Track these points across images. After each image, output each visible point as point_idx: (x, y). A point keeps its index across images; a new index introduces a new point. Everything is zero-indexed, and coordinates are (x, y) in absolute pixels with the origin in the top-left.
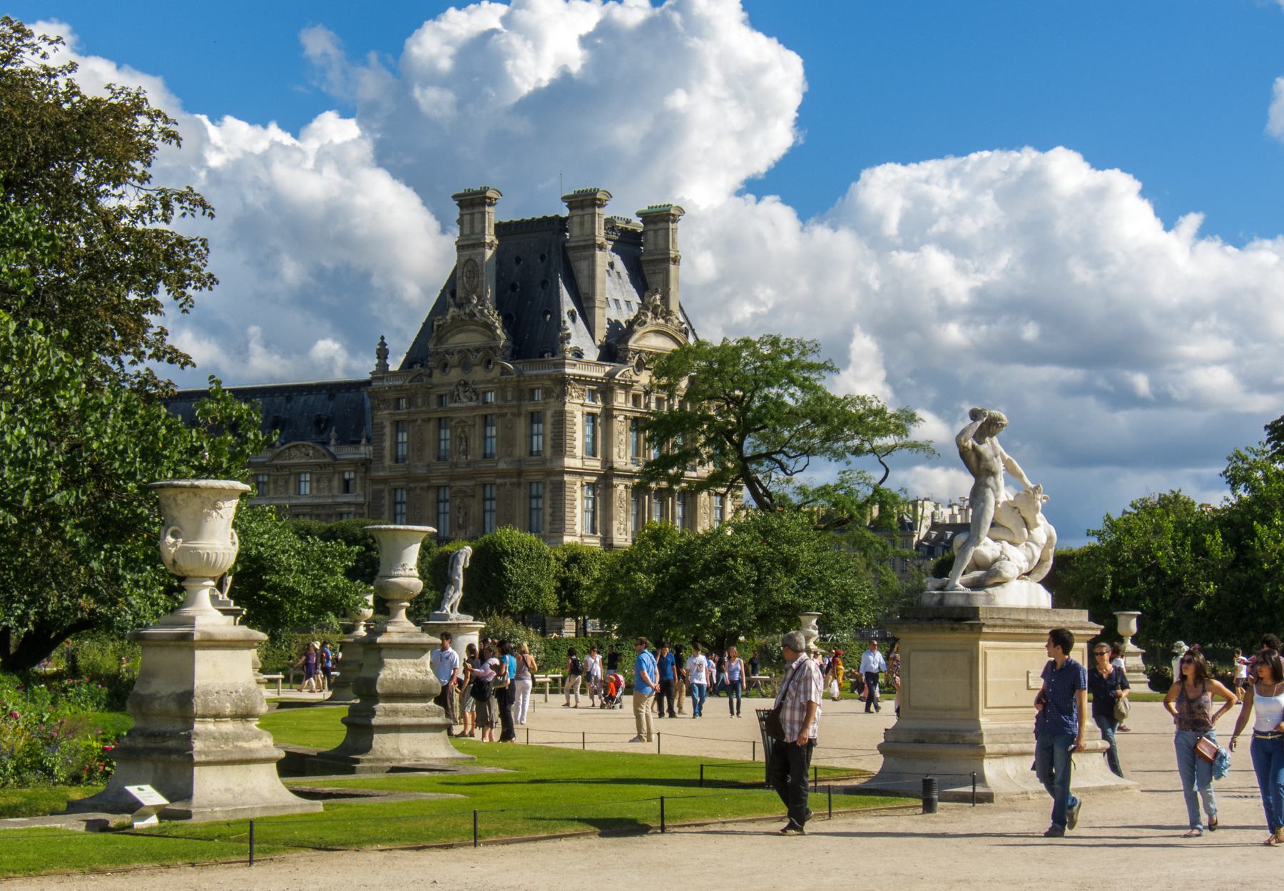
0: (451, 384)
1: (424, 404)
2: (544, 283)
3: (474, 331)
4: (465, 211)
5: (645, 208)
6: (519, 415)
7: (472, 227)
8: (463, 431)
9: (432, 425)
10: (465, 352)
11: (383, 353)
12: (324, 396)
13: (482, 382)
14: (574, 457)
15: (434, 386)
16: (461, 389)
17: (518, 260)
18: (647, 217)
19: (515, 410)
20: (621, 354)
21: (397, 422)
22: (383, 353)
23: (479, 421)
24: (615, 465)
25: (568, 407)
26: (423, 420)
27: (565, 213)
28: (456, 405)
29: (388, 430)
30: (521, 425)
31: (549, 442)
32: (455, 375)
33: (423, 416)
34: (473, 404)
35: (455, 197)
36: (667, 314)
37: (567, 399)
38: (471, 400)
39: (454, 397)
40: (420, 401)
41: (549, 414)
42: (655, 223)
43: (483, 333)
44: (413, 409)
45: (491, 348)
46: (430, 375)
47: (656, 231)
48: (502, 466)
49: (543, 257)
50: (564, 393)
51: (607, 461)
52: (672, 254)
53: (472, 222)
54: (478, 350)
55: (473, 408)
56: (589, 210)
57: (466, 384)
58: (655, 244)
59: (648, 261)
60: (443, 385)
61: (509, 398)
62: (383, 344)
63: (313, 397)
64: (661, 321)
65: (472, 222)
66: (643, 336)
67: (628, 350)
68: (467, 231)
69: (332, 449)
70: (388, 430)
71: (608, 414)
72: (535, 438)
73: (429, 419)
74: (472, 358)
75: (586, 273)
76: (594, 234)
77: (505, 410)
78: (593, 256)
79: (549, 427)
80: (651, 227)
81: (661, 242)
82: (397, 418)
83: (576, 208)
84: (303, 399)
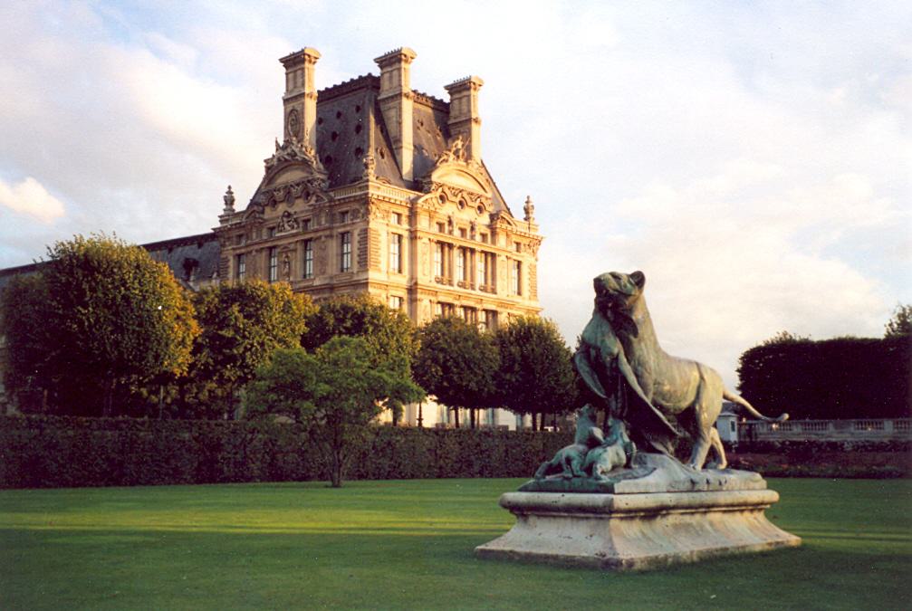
0: (278, 218)
1: (257, 237)
2: (358, 128)
3: (296, 169)
4: (290, 70)
5: (450, 82)
6: (331, 236)
7: (295, 83)
8: (287, 257)
9: (264, 254)
10: (287, 189)
11: (229, 200)
12: (195, 246)
13: (302, 212)
14: (379, 270)
15: (265, 221)
16: (285, 219)
17: (339, 115)
18: (452, 89)
19: (328, 233)
20: (426, 187)
21: (239, 256)
22: (229, 200)
23: (300, 247)
24: (419, 282)
25: (372, 225)
26: (257, 251)
27: (376, 72)
28: (283, 234)
29: (231, 263)
30: (333, 245)
31: (356, 259)
32: (282, 208)
33: (256, 247)
34: (294, 231)
35: (281, 60)
36: (468, 158)
37: (371, 217)
38: (293, 228)
39: (280, 227)
40: (254, 235)
41: (356, 232)
42: (460, 92)
43: (303, 170)
44: (249, 242)
45: (309, 181)
46: (263, 212)
47: (460, 98)
48: (317, 283)
49: (358, 109)
50: (368, 212)
51: (413, 278)
52: (474, 116)
53: (295, 77)
54: (298, 185)
55: (294, 235)
56: (397, 66)
57: (289, 215)
58: (460, 110)
59: (454, 124)
60: (273, 219)
61: (323, 223)
62: (230, 192)
63: (187, 248)
64: (461, 162)
65: (295, 77)
66: (446, 174)
67: (431, 183)
68: (291, 87)
69: (191, 284)
70: (231, 263)
71: (413, 237)
72: (345, 256)
73: (262, 249)
74: (293, 190)
75: (394, 119)
76: (400, 86)
77: (319, 234)
78: (400, 103)
79: (356, 245)
80: (457, 96)
81: (465, 108)
82: (238, 252)
83: (386, 66)
84: (180, 249)
